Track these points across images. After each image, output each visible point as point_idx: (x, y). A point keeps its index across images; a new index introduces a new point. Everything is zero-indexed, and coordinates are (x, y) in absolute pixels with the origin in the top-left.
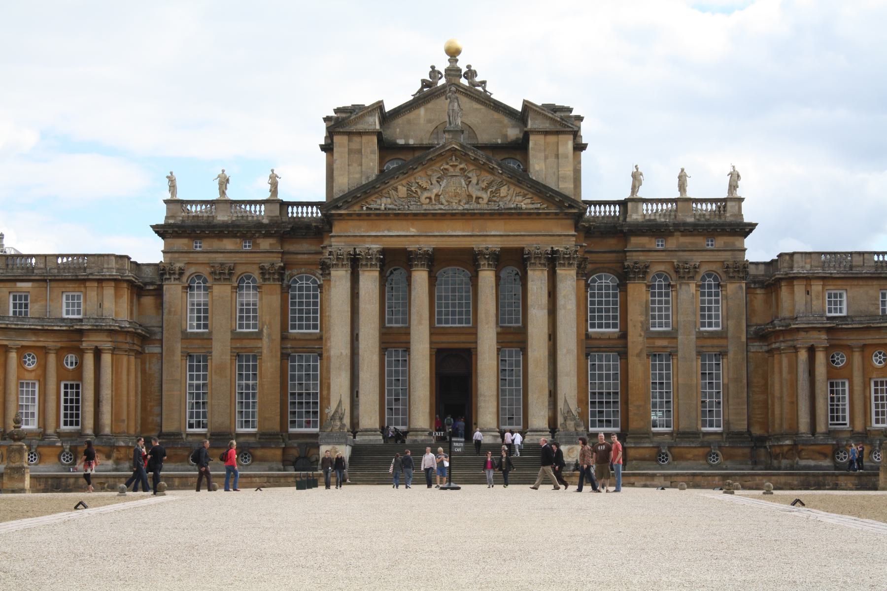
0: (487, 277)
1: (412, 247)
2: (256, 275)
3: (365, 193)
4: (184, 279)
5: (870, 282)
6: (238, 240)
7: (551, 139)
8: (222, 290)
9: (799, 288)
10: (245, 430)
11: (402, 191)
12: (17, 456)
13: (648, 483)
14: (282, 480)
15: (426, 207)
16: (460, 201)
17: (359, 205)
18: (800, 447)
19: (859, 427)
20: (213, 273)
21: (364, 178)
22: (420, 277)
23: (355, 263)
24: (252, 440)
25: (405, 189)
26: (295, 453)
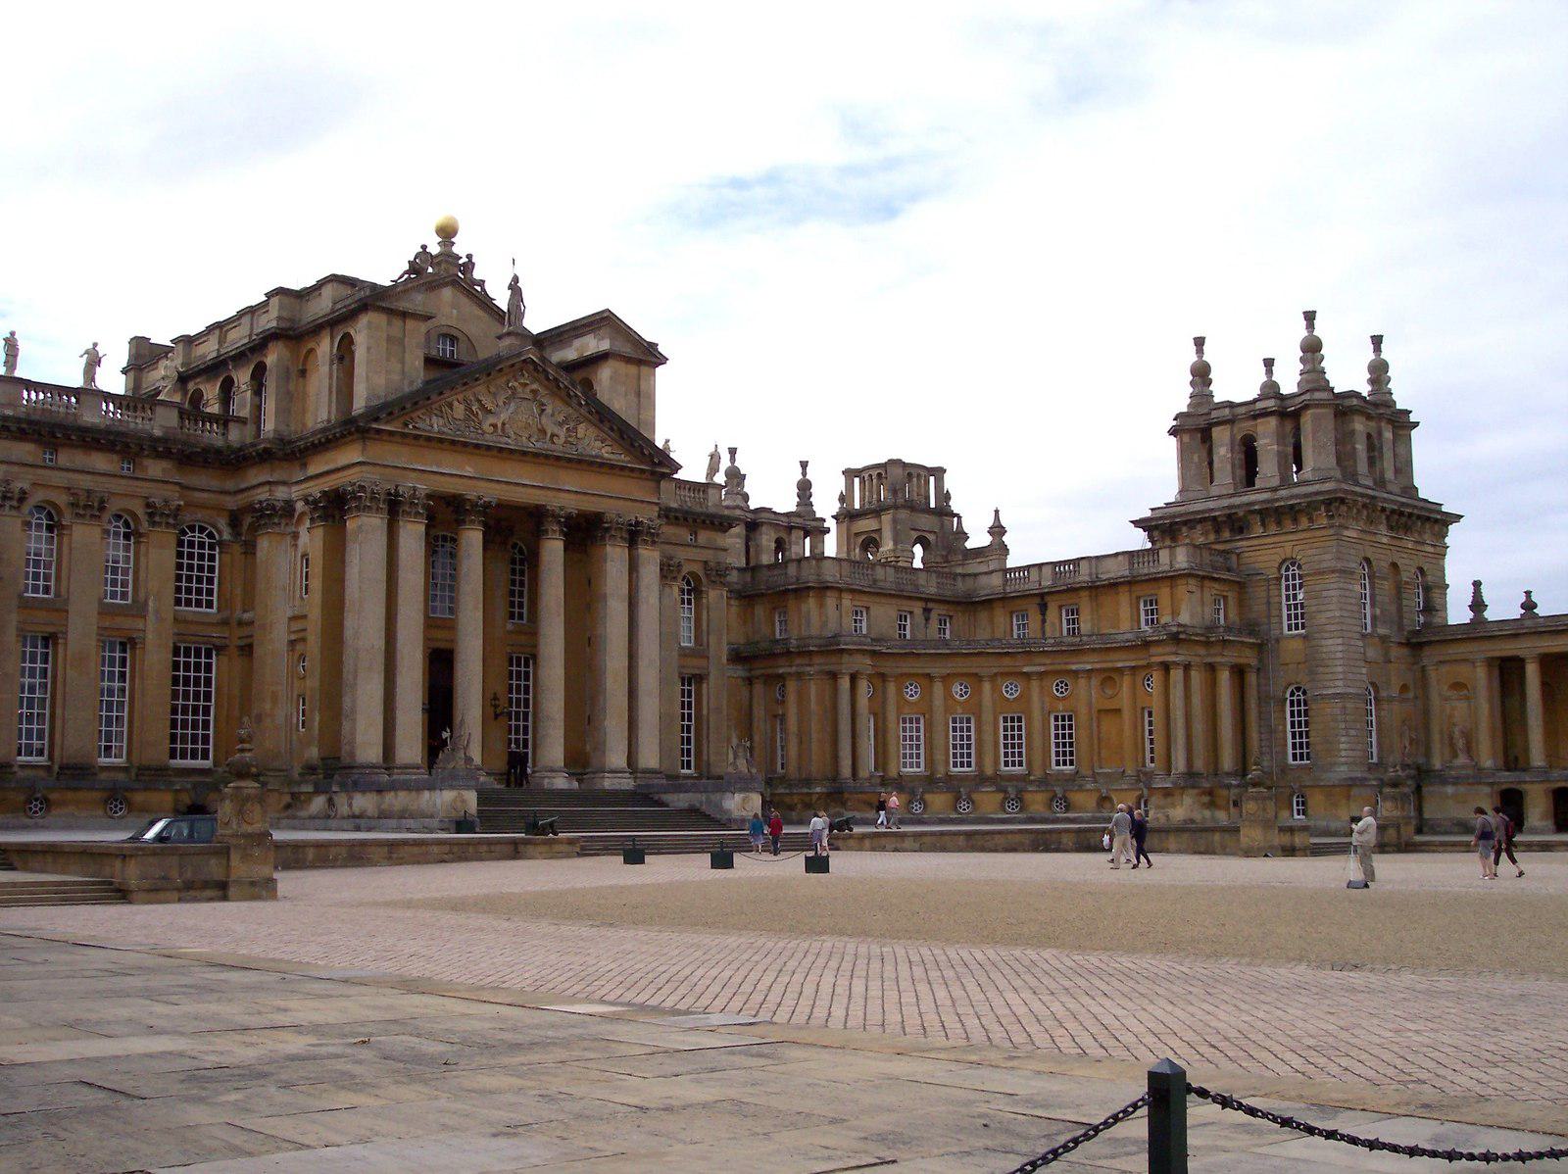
0: (553, 550)
1: (472, 495)
2: (140, 512)
3: (416, 403)
4: (26, 508)
5: (890, 600)
6: (115, 457)
7: (632, 369)
8: (84, 534)
9: (831, 601)
10: (104, 761)
11: (459, 410)
12: (257, 808)
13: (899, 846)
14: (484, 848)
15: (490, 439)
16: (530, 436)
17: (402, 420)
18: (846, 795)
19: (893, 773)
20: (74, 505)
21: (406, 382)
22: (473, 539)
23: (394, 507)
24: (121, 776)
25: (462, 407)
26: (186, 799)
